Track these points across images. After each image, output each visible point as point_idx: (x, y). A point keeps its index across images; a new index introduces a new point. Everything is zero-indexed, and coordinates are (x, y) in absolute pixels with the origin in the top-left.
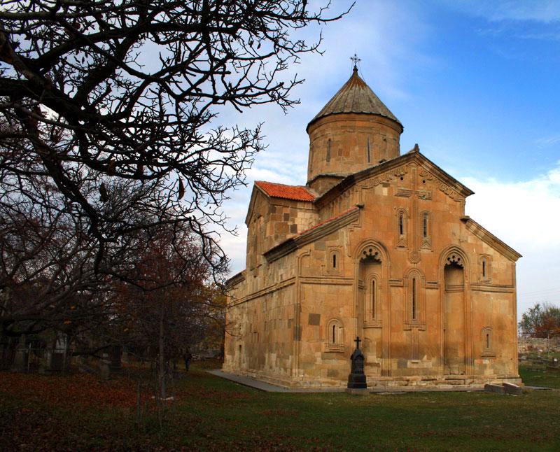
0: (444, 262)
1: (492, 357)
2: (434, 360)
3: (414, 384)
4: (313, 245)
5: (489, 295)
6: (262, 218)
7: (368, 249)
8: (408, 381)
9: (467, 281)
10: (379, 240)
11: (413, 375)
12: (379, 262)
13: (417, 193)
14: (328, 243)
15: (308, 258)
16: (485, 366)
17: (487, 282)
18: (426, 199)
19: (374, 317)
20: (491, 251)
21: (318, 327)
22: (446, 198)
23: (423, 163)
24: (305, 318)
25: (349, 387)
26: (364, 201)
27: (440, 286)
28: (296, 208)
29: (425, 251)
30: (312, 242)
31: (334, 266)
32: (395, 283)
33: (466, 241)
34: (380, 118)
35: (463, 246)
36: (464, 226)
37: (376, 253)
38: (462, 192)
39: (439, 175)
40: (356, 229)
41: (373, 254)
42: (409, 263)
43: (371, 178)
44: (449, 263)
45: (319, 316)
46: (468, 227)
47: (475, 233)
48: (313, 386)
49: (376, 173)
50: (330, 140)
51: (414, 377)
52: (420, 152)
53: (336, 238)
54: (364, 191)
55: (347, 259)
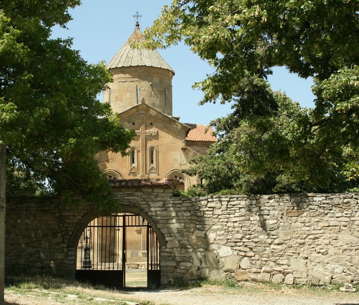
8: (138, 265)
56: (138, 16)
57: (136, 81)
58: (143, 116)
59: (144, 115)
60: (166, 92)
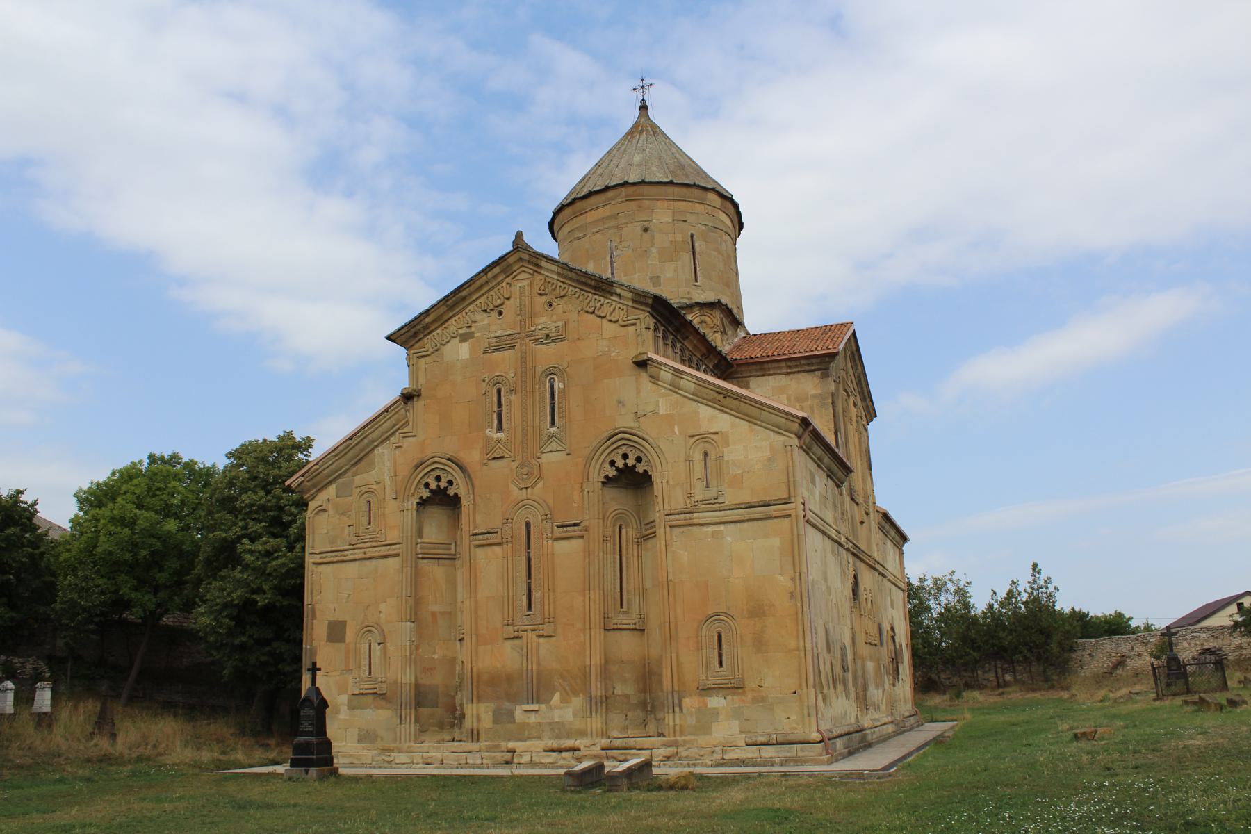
1: (736, 688)
2: (578, 702)
3: (526, 758)
4: (331, 491)
5: (720, 532)
8: (513, 751)
10: (451, 453)
11: (529, 738)
13: (529, 334)
14: (358, 480)
15: (326, 513)
16: (715, 713)
17: (712, 504)
18: (554, 341)
21: (343, 644)
22: (601, 328)
23: (540, 267)
30: (330, 483)
31: (370, 524)
32: (487, 539)
34: (631, 190)
35: (649, 429)
36: (644, 377)
38: (634, 301)
39: (578, 281)
41: (443, 484)
44: (612, 472)
45: (346, 621)
46: (654, 379)
47: (675, 388)
51: (528, 743)
54: (423, 361)
55: (391, 506)
57: (608, 228)
59: (525, 283)
60: (697, 245)
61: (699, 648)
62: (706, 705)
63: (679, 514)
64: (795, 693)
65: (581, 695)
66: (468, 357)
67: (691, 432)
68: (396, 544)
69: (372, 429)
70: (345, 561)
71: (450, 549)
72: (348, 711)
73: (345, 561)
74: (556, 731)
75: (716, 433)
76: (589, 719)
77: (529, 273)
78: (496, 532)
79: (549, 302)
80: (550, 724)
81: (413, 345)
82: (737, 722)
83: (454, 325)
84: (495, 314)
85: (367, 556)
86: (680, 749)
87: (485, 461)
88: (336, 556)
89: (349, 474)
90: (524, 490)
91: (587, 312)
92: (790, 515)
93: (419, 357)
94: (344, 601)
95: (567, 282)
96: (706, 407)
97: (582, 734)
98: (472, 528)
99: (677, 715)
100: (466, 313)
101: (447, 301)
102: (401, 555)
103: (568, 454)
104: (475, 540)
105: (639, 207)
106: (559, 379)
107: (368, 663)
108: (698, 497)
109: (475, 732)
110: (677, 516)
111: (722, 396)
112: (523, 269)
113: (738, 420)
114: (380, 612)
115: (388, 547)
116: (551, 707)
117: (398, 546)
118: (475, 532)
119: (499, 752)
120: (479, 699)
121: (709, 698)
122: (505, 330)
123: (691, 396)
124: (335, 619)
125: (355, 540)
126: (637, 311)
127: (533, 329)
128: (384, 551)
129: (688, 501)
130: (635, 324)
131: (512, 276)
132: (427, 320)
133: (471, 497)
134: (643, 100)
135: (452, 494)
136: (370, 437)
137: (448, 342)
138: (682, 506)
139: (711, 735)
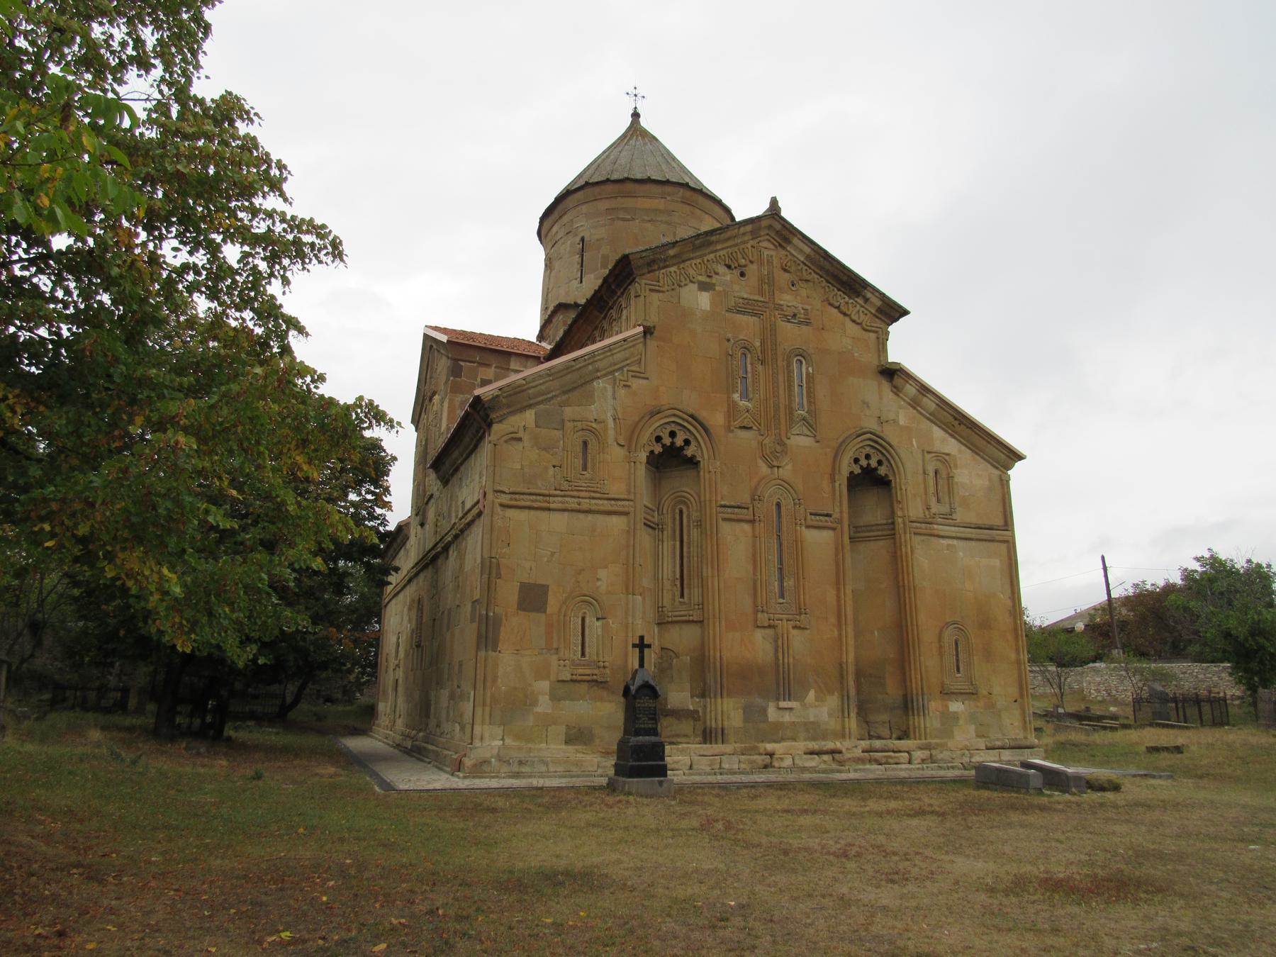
0: (846, 467)
1: (972, 694)
3: (788, 762)
4: (530, 416)
6: (436, 398)
7: (667, 432)
8: (771, 755)
9: (900, 513)
10: (690, 411)
11: (783, 739)
12: (693, 463)
13: (779, 307)
14: (568, 412)
15: (521, 444)
16: (955, 717)
18: (800, 323)
19: (682, 596)
20: (951, 446)
21: (542, 617)
24: (508, 593)
25: (617, 773)
26: (653, 319)
27: (840, 521)
28: (508, 369)
29: (800, 441)
30: (530, 406)
31: (585, 468)
33: (895, 422)
34: (688, 193)
35: (890, 434)
36: (886, 386)
37: (687, 442)
39: (827, 272)
40: (636, 383)
41: (679, 442)
42: (764, 469)
43: (672, 269)
44: (857, 470)
45: (544, 589)
46: (897, 390)
47: (914, 404)
48: (524, 769)
49: (680, 259)
50: (583, 239)
52: (783, 214)
53: (589, 399)
54: (655, 296)
55: (617, 453)
56: (636, 95)
57: (661, 221)
58: (772, 256)
61: (941, 654)
62: (947, 707)
63: (921, 523)
64: (1016, 701)
65: (836, 693)
66: (709, 309)
67: (928, 449)
68: (624, 500)
69: (602, 356)
70: (549, 509)
71: (654, 517)
72: (550, 703)
73: (549, 509)
74: (811, 731)
75: (948, 454)
76: (847, 719)
77: (774, 244)
78: (748, 508)
79: (792, 282)
80: (805, 724)
81: (643, 274)
82: (973, 726)
83: (691, 268)
84: (737, 272)
85: (585, 507)
86: (934, 752)
87: (732, 428)
88: (536, 501)
89: (554, 401)
90: (776, 469)
91: (831, 305)
92: (1007, 542)
93: (651, 290)
94: (545, 559)
95: (813, 267)
96: (938, 428)
97: (842, 735)
98: (719, 498)
99: (927, 717)
100: (708, 261)
101: (698, 239)
102: (632, 515)
103: (817, 442)
104: (722, 513)
105: (692, 213)
106: (806, 364)
107: (580, 642)
108: (933, 511)
109: (726, 731)
110: (919, 525)
111: (957, 422)
112: (768, 237)
113: (963, 448)
114: (598, 580)
115: (613, 502)
116: (805, 704)
117: (627, 503)
118: (723, 503)
119: (757, 754)
120: (728, 695)
121: (950, 703)
122: (751, 294)
123: (928, 415)
124: (531, 581)
125: (565, 485)
126: (877, 320)
127: (782, 303)
128: (606, 505)
129: (927, 512)
130: (876, 332)
131: (757, 240)
132: (671, 252)
133: (718, 463)
134: (636, 108)
135: (689, 456)
136: (597, 365)
137: (686, 285)
138: (921, 515)
139: (953, 738)
